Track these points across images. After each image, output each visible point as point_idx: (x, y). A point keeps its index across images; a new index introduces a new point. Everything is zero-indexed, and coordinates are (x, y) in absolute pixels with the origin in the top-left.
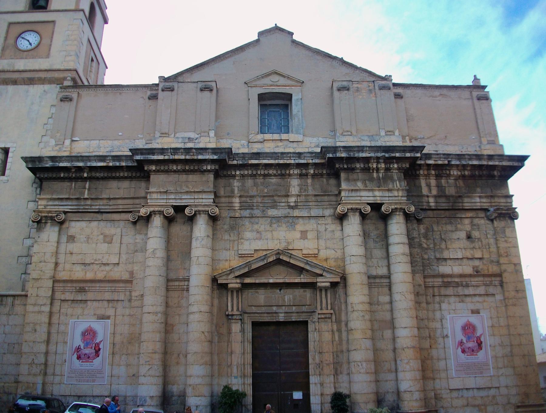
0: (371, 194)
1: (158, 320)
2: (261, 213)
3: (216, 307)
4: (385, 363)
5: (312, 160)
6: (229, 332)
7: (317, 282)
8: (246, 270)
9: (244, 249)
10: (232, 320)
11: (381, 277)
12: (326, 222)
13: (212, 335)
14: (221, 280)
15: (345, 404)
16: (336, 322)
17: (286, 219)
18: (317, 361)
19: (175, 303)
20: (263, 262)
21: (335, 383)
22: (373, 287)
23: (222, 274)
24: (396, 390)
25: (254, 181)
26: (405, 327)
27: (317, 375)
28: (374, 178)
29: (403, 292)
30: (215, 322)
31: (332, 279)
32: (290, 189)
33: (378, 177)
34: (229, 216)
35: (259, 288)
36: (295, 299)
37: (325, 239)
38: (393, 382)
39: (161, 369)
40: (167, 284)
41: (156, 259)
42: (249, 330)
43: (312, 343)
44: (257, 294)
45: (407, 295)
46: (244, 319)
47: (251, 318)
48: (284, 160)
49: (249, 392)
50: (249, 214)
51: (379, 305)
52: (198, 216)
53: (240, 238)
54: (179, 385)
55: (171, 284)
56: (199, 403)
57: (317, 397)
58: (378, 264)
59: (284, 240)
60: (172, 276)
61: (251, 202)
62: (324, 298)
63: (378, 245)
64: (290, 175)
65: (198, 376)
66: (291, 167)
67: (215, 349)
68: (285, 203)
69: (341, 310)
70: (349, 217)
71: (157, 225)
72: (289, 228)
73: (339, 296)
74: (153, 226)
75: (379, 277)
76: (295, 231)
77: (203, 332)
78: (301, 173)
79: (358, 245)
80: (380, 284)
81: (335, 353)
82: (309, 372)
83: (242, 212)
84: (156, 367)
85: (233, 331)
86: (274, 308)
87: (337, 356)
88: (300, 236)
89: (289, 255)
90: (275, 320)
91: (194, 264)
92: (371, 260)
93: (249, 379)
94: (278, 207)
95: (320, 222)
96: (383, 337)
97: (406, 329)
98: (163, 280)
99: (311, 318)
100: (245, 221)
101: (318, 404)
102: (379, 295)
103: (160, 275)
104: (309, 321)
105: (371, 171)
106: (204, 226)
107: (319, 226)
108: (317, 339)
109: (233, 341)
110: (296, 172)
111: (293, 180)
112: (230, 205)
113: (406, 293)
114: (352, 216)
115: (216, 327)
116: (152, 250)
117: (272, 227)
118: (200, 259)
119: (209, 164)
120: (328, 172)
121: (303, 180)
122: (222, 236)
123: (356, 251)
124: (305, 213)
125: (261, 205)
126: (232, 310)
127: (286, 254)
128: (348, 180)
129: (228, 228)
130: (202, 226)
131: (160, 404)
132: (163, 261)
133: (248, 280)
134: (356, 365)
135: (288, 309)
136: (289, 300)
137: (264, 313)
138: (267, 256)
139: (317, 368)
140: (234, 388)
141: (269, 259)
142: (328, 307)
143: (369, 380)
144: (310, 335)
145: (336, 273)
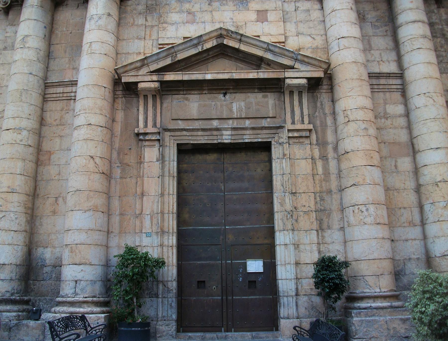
1: (21, 141)
3: (120, 124)
4: (402, 210)
6: (140, 162)
7: (285, 78)
8: (168, 61)
9: (166, 37)
10: (144, 142)
11: (389, 76)
14: (127, 78)
15: (340, 277)
18: (288, 207)
19: (56, 120)
20: (196, 48)
21: (319, 244)
22: (376, 90)
23: (129, 68)
24: (424, 256)
26: (437, 148)
27: (287, 230)
29: (429, 93)
30: (117, 146)
31: (310, 73)
35: (189, 92)
36: (249, 108)
37: (295, 23)
38: (417, 242)
39: (23, 219)
40: (45, 91)
41: (26, 50)
42: (172, 158)
43: (279, 178)
44: (186, 102)
45: (436, 97)
46: (163, 140)
47: (175, 138)
49: (170, 259)
51: (387, 119)
54: (55, 247)
55: (51, 90)
57: (288, 267)
58: (381, 58)
60: (53, 78)
62: (297, 106)
65: (80, 230)
67: (116, 189)
69: (326, 126)
71: (32, 3)
72: (238, 6)
74: (27, 5)
75: (385, 75)
76: (248, 10)
77: (92, 157)
79: (351, 22)
80: (387, 87)
82: (273, 227)
84: (12, 215)
85: (147, 159)
86: (215, 124)
87: (322, 199)
89: (239, 37)
90: (215, 142)
91: (85, 53)
92: (370, 53)
93: (171, 238)
96: (396, 168)
97: (439, 150)
98: (36, 81)
99: (276, 138)
101: (291, 279)
102: (385, 104)
103: (31, 74)
104: (273, 143)
107: (286, 5)
108: (287, 170)
109: (146, 176)
113: (434, 94)
115: (119, 154)
116: (22, 37)
117: (211, 5)
118: (94, 45)
123: (348, 31)
126: (146, 126)
127: (234, 36)
129: (144, 9)
131: (17, 277)
132: (38, 53)
133: (170, 77)
134: (356, 211)
135: (237, 124)
136: (240, 109)
137: (198, 130)
139: (287, 219)
141: (206, 44)
142: (305, 119)
143: (381, 236)
144: (275, 165)
145: (316, 63)
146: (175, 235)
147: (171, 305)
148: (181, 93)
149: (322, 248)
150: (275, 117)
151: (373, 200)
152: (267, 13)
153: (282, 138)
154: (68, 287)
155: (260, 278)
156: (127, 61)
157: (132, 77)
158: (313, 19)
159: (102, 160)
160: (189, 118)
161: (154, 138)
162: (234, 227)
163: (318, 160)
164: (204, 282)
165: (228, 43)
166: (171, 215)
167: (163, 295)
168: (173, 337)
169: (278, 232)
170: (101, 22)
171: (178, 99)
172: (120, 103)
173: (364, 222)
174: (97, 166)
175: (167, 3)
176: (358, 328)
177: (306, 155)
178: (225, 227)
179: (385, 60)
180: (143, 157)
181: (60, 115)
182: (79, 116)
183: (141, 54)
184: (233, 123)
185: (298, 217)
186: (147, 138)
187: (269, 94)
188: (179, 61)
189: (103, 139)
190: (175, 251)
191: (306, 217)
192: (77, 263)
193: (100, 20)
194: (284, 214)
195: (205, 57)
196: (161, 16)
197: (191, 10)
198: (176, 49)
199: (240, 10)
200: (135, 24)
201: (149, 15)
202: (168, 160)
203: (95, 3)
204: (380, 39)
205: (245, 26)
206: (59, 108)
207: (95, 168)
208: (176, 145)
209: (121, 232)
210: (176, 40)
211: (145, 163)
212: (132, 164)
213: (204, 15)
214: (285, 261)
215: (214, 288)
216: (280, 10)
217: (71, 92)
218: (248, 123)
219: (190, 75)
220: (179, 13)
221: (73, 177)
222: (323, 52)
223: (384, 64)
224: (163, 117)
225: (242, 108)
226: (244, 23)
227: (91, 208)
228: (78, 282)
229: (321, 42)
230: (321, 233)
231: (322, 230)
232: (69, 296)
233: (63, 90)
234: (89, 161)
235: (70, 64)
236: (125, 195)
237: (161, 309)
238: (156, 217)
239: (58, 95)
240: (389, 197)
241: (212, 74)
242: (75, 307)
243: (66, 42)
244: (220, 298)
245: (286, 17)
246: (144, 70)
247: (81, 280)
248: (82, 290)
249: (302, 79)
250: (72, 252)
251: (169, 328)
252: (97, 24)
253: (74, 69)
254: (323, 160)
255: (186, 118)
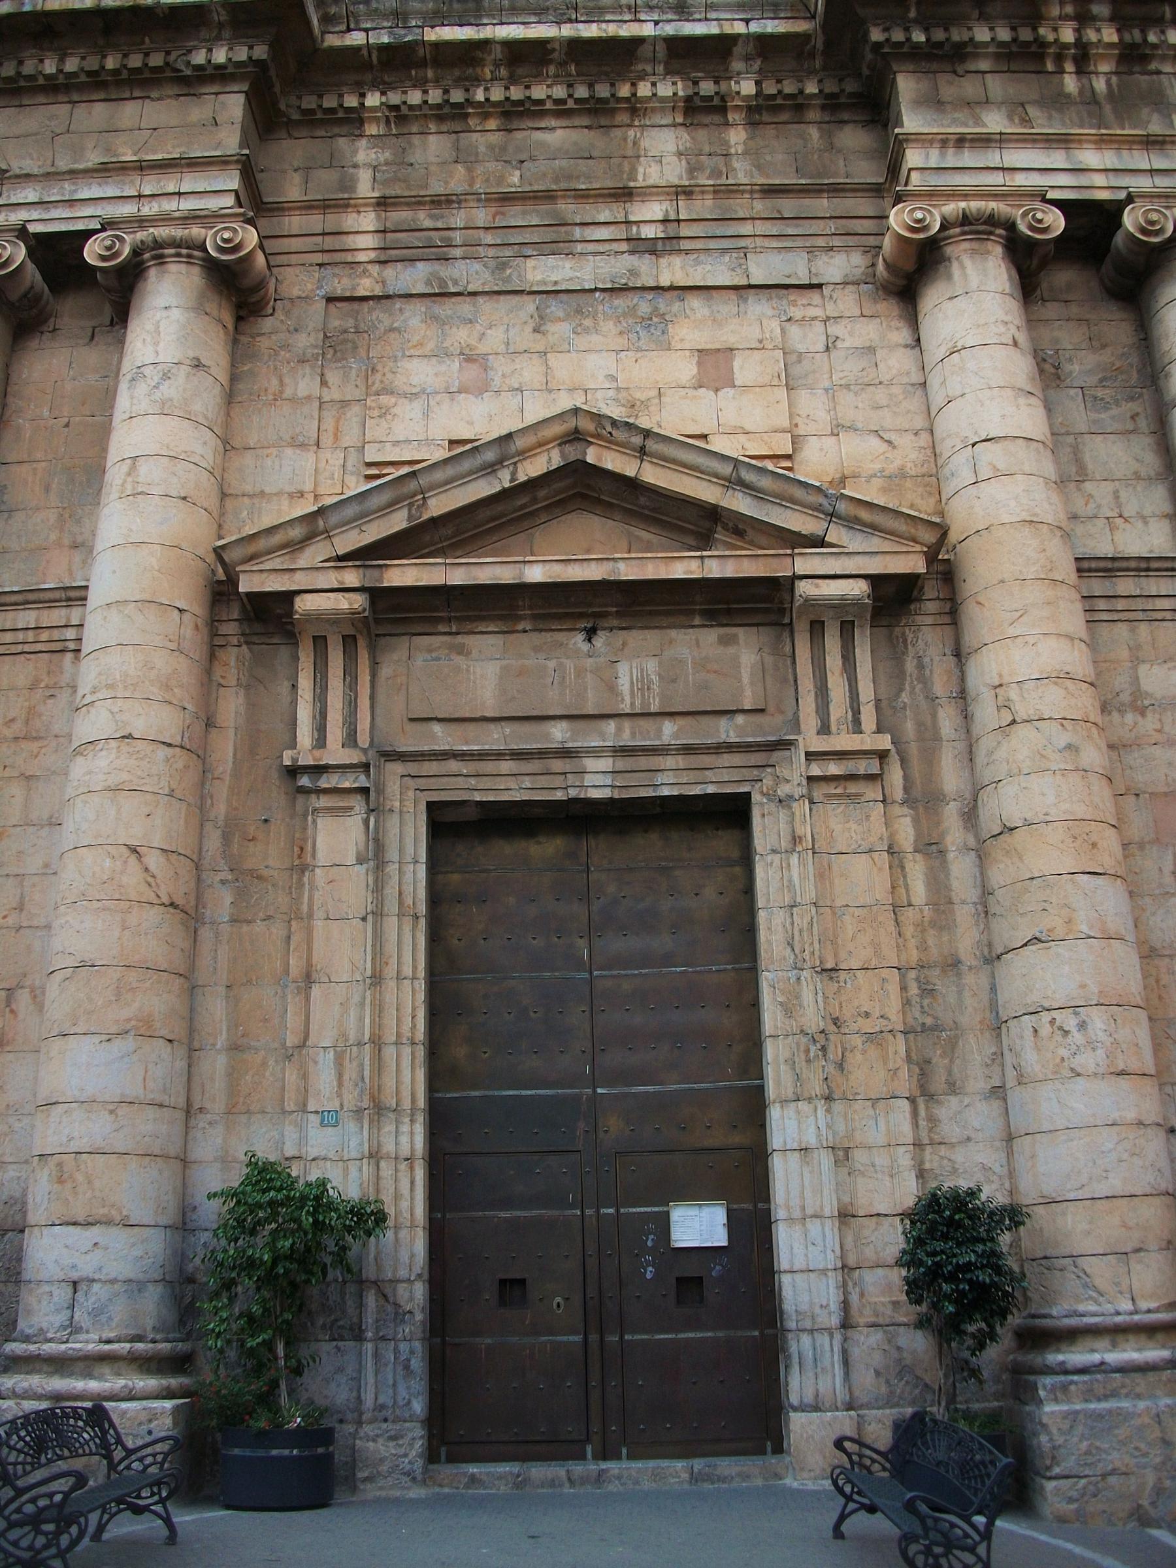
0: (1057, 159)
2: (487, 275)
3: (231, 732)
5: (747, 21)
7: (796, 577)
8: (398, 522)
9: (390, 438)
10: (313, 796)
12: (831, 310)
13: (199, 880)
14: (256, 578)
15: (993, 1260)
16: (909, 801)
17: (616, 302)
18: (812, 1017)
20: (490, 478)
21: (918, 1145)
22: (1104, 616)
23: (262, 544)
25: (458, 140)
27: (810, 1100)
28: (1068, 96)
30: (220, 809)
31: (879, 558)
32: (641, 170)
33: (1089, 94)
34: (322, 292)
35: (469, 626)
36: (674, 681)
37: (827, 390)
42: (410, 850)
43: (780, 917)
44: (460, 660)
46: (380, 791)
47: (422, 783)
48: (604, 25)
49: (405, 1204)
50: (428, 283)
51: (1143, 714)
52: (152, 273)
53: (374, 389)
56: (86, 1266)
57: (814, 1227)
58: (1119, 506)
59: (611, 393)
61: (440, 225)
63: (1113, 418)
64: (635, 108)
65: (88, 1103)
66: (640, 67)
67: (215, 958)
68: (612, 228)
69: (937, 738)
70: (955, 265)
72: (633, 336)
73: (920, 666)
75: (1133, 564)
77: (134, 850)
78: (690, 92)
80: (1140, 604)
81: (912, 974)
82: (761, 1089)
83: (389, 272)
85: (322, 857)
86: (559, 733)
87: (927, 991)
88: (695, 371)
89: (637, 440)
90: (559, 795)
91: (114, 495)
93: (405, 1128)
94: (579, 248)
95: (797, 313)
99: (768, 782)
100: (407, 314)
101: (824, 1272)
102: (1137, 661)
104: (756, 797)
105: (1050, 67)
106: (176, 314)
107: (794, 330)
108: (808, 892)
109: (319, 914)
110: (665, 90)
111: (654, 132)
112: (330, 242)
114: (967, 261)
115: (226, 838)
118: (144, 468)
119: (219, 38)
120: (827, 91)
121: (702, 134)
122: (281, 381)
124: (718, 272)
125: (489, 238)
126: (320, 741)
127: (620, 435)
128: (934, 102)
129: (316, 347)
130: (165, 313)
134: (1045, 1031)
135: (633, 734)
137: (499, 755)
138: (513, 449)
139: (808, 1061)
140: (306, 1174)
141: (526, 463)
142: (863, 717)
143: (1131, 1115)
144: (766, 876)
145: (900, 526)
146: (420, 1118)
147: (407, 1367)
148: (442, 628)
149: (931, 1161)
150: (762, 711)
151: (1101, 992)
152: (732, 360)
153: (788, 781)
154: (45, 1303)
155: (718, 1268)
156: (256, 520)
157: (273, 576)
158: (888, 377)
159: (168, 860)
160: (467, 715)
161: (347, 785)
162: (626, 1089)
163: (909, 856)
164: (522, 1282)
165: (600, 459)
166: (407, 1051)
167: (378, 1329)
168: (414, 1479)
169: (778, 1105)
170: (169, 390)
171: (430, 651)
172: (232, 663)
173: (1072, 1070)
174: (150, 879)
175: (395, 325)
176: (1060, 1440)
177: (871, 839)
178: (595, 1091)
179: (1134, 514)
180: (309, 848)
181: (27, 704)
182: (91, 709)
183: (306, 495)
184: (619, 730)
185: (847, 1054)
186: (325, 782)
187: (740, 632)
188: (433, 521)
189: (174, 787)
190: (420, 1174)
191: (873, 1052)
192: (81, 1219)
193: (168, 382)
194: (798, 1044)
195: (522, 507)
196: (373, 369)
197: (476, 348)
198: (424, 481)
199: (639, 350)
200: (285, 396)
201: (333, 365)
202: (396, 858)
203: (149, 326)
204: (1114, 442)
205: (657, 401)
206: (22, 681)
207: (144, 888)
208: (423, 807)
209: (234, 1110)
210: (424, 449)
211: (317, 871)
212: (272, 872)
213: (518, 367)
214: (803, 1208)
215: (558, 1305)
216: (775, 348)
217: (66, 626)
218: (669, 731)
219: (472, 568)
220: (434, 359)
221: (68, 918)
222: (920, 489)
223: (1128, 525)
224: (378, 711)
225: (651, 681)
226: (654, 393)
227: (128, 1027)
228: (83, 1287)
229: (913, 455)
230: (927, 1108)
231: (930, 1096)
232: (50, 1335)
233: (37, 620)
234: (125, 862)
235: (62, 530)
236: (249, 981)
237: (371, 1380)
238: (354, 1055)
239: (20, 636)
240: (1157, 981)
241: (548, 566)
242: (71, 1375)
243: (50, 457)
244: (578, 1338)
245: (796, 370)
246: (316, 553)
247: (94, 1280)
248: (96, 1313)
249: (851, 581)
250: (60, 1181)
251: (401, 1446)
252: (157, 395)
253: (75, 546)
254: (927, 855)
255: (456, 716)
